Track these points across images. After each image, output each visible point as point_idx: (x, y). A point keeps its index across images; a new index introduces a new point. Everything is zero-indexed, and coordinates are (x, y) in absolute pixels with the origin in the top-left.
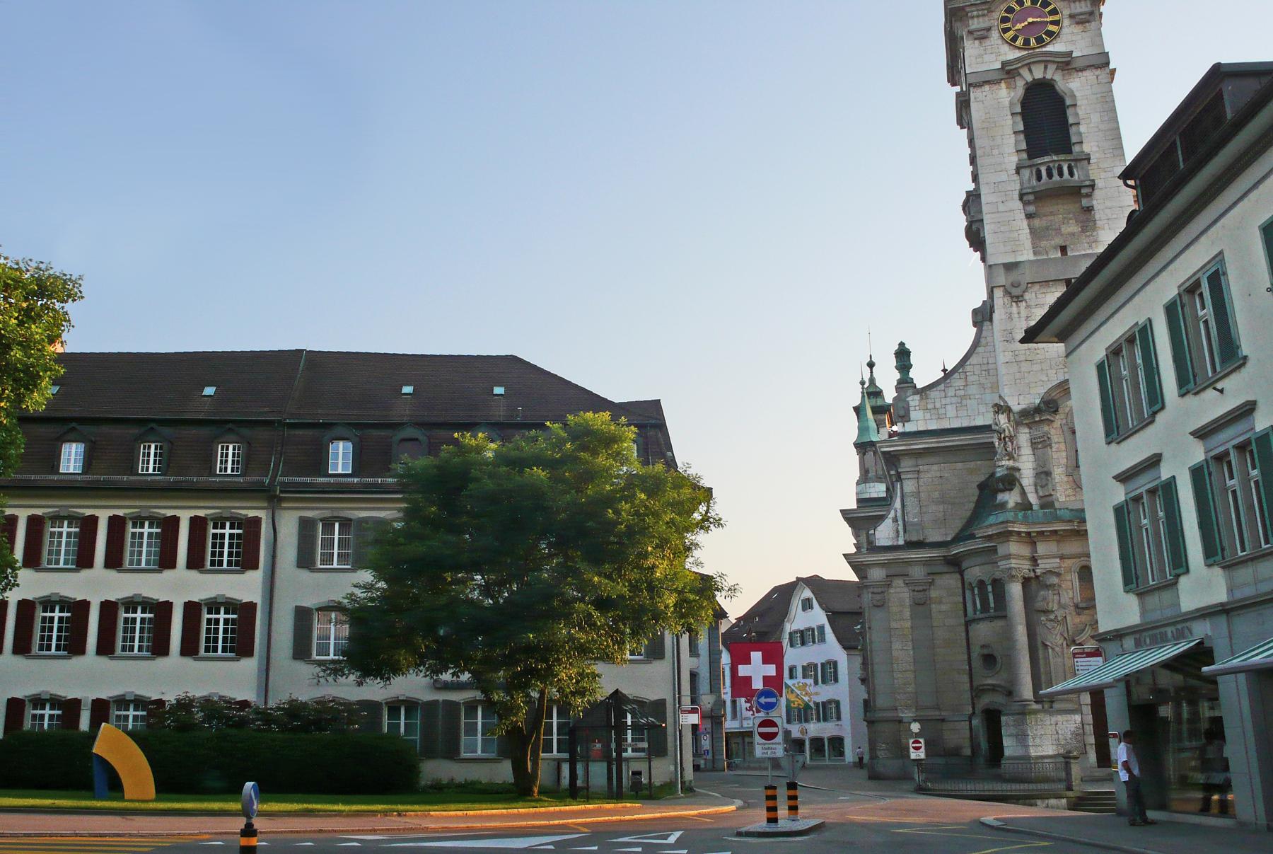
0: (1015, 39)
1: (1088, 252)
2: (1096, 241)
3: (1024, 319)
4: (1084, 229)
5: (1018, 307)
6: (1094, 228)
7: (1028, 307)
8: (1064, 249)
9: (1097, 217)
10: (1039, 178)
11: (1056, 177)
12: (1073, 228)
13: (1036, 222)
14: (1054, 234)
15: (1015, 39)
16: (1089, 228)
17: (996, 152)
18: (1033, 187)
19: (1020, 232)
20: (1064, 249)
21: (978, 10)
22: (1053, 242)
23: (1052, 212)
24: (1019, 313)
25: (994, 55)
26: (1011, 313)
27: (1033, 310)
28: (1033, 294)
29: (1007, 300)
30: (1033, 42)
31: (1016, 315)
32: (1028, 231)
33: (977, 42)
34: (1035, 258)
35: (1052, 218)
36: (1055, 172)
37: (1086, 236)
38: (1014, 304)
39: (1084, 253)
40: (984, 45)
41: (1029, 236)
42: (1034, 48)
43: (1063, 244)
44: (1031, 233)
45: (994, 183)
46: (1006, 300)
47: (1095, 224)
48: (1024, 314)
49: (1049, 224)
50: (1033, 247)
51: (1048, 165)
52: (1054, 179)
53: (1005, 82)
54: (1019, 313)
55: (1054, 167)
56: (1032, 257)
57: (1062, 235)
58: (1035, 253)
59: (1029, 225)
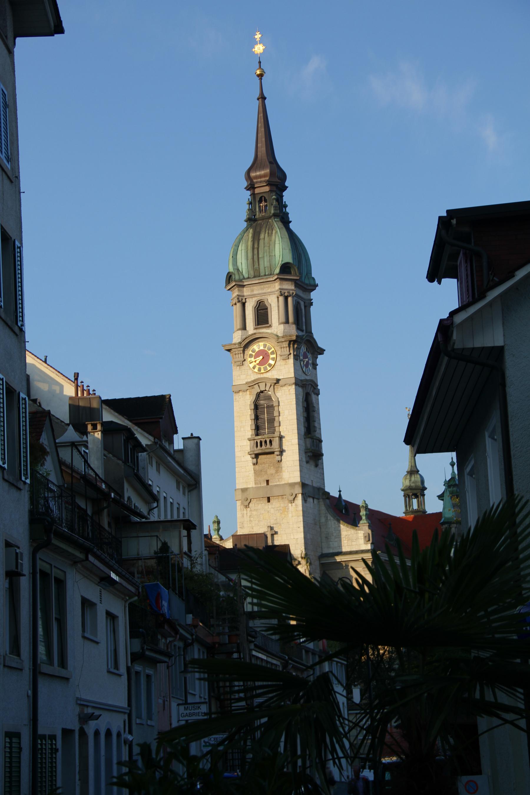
0: (254, 368)
1: (278, 483)
2: (281, 478)
3: (248, 517)
4: (277, 472)
5: (247, 510)
6: (281, 472)
7: (251, 510)
8: (268, 481)
9: (283, 465)
10: (257, 446)
11: (263, 447)
12: (272, 471)
13: (257, 467)
14: (264, 474)
15: (254, 368)
16: (279, 471)
17: (242, 429)
18: (254, 451)
19: (250, 472)
20: (268, 481)
21: (238, 351)
22: (263, 478)
23: (264, 462)
24: (247, 514)
25: (245, 375)
26: (243, 514)
27: (253, 512)
28: (253, 504)
29: (242, 507)
30: (262, 371)
31: (246, 515)
32: (253, 472)
33: (238, 367)
34: (255, 486)
35: (263, 465)
36: (263, 443)
37: (277, 475)
38: (245, 509)
39: (276, 484)
40: (241, 369)
41: (253, 475)
42: (263, 373)
43: (268, 479)
44: (254, 472)
45: (241, 446)
46: (242, 507)
47: (282, 469)
48: (248, 515)
49: (262, 469)
50: (255, 481)
51: (260, 439)
52: (262, 447)
53: (249, 391)
54: (247, 514)
55: (263, 441)
56: (254, 486)
57: (267, 475)
58: (255, 484)
59: (254, 469)
